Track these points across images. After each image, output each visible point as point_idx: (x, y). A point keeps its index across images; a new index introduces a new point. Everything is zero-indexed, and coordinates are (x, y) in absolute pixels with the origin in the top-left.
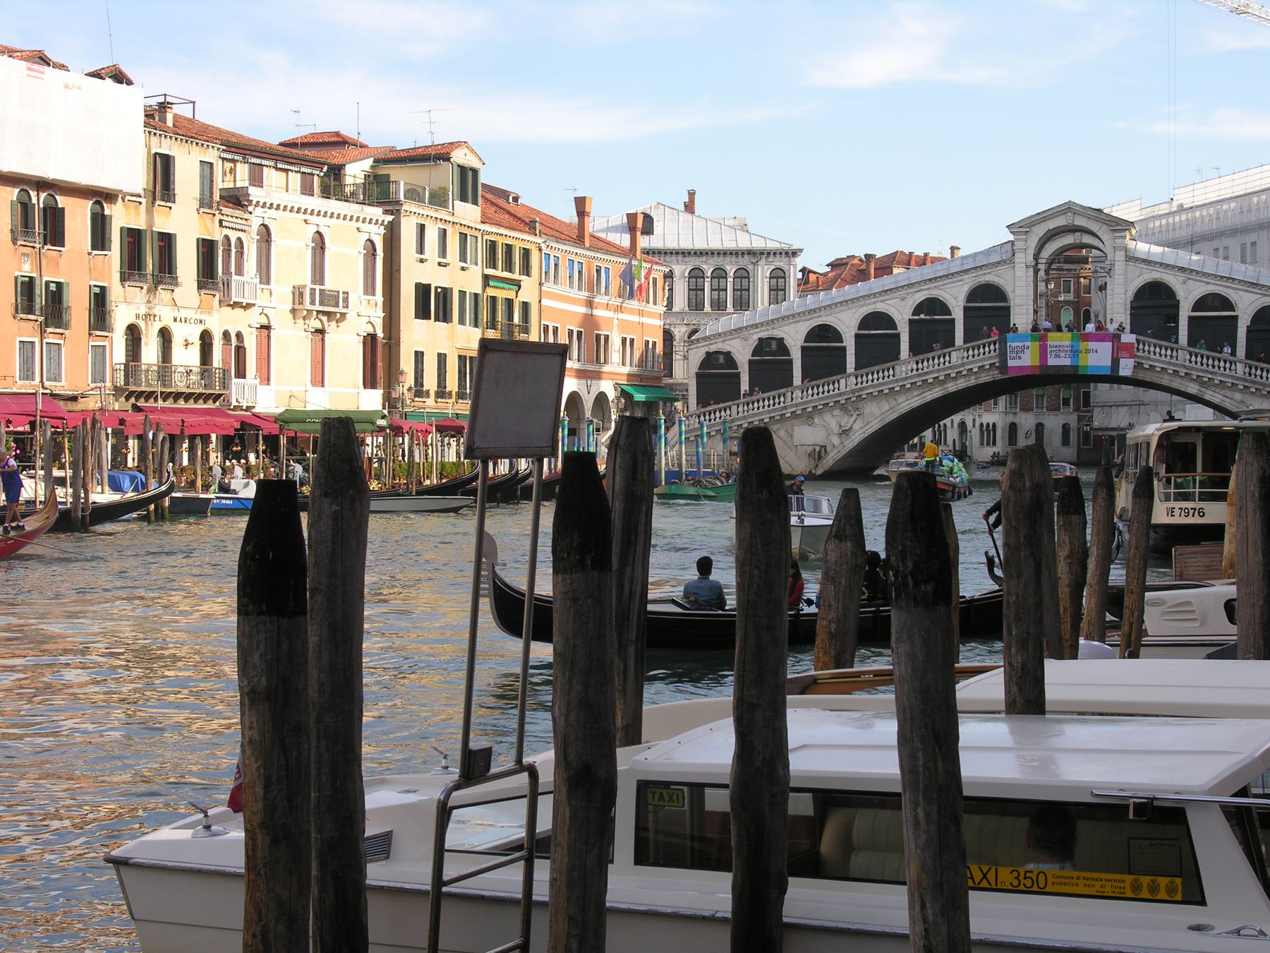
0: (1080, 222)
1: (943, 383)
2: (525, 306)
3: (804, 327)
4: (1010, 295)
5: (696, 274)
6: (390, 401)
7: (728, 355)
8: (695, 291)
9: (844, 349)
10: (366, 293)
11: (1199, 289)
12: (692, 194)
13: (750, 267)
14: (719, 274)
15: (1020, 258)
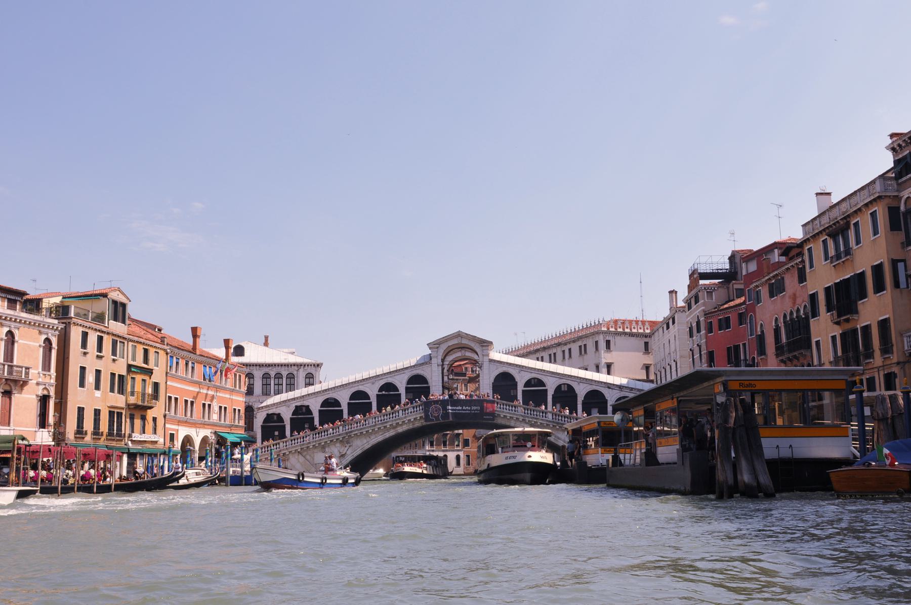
0: (465, 342)
1: (394, 428)
2: (156, 386)
3: (321, 399)
4: (429, 380)
5: (266, 376)
6: (59, 437)
7: (279, 415)
8: (266, 385)
9: (342, 411)
10: (44, 369)
11: (528, 376)
12: (266, 338)
13: (295, 373)
14: (279, 376)
15: (434, 361)
